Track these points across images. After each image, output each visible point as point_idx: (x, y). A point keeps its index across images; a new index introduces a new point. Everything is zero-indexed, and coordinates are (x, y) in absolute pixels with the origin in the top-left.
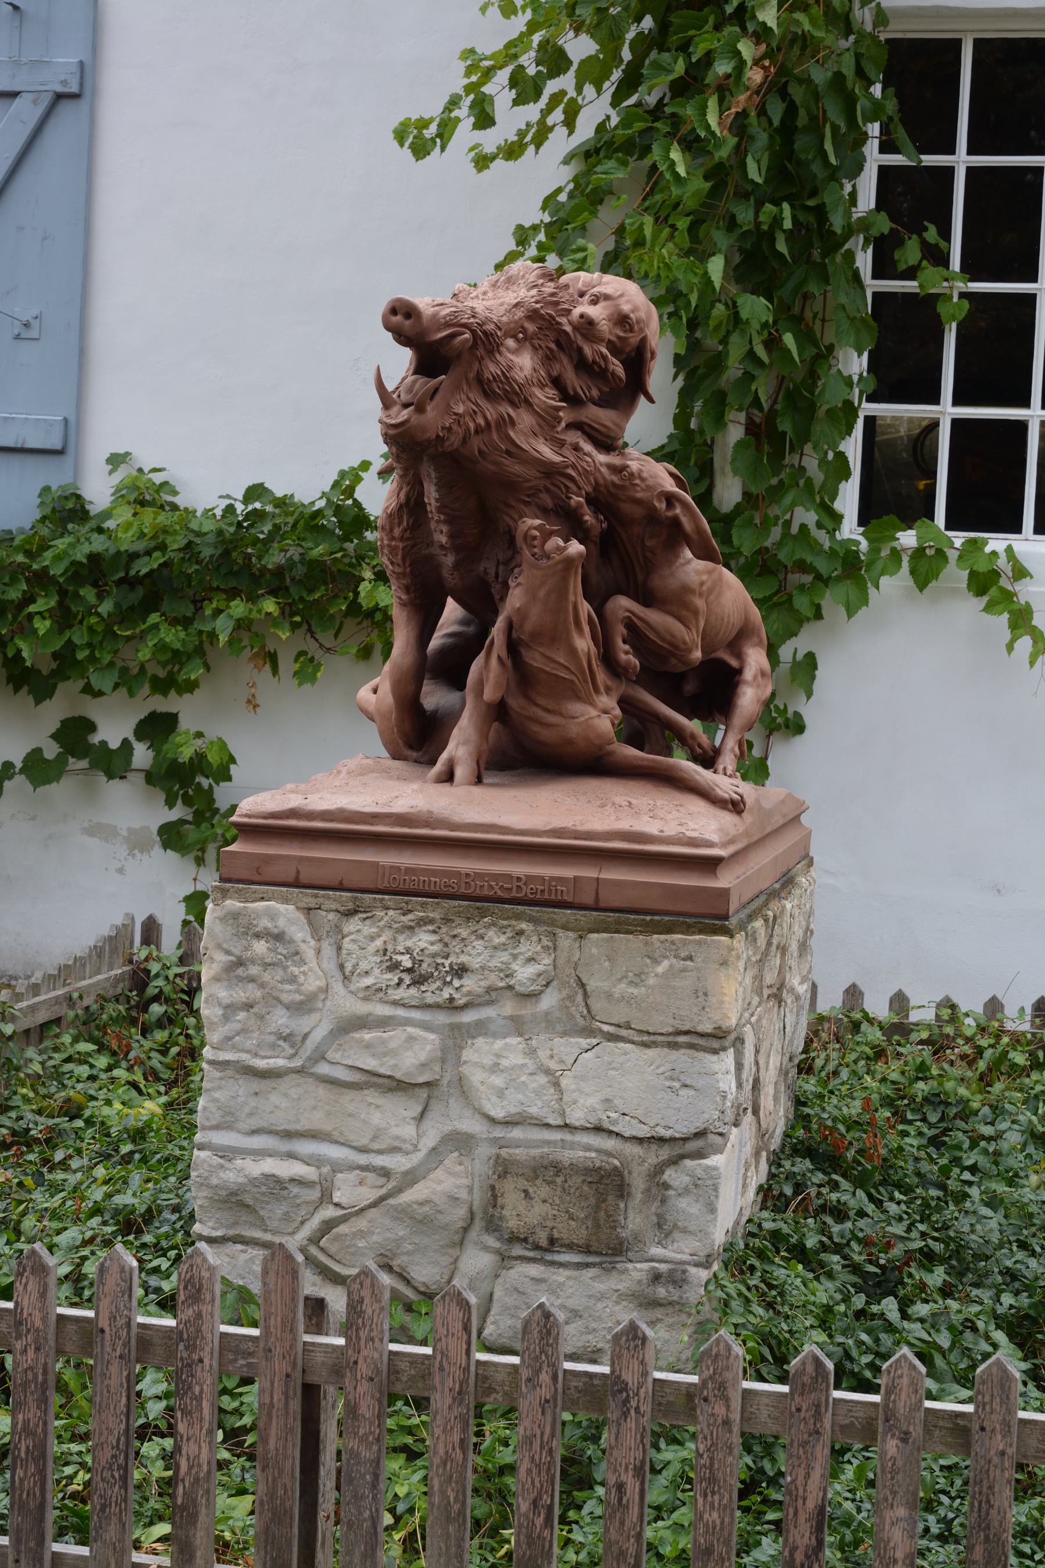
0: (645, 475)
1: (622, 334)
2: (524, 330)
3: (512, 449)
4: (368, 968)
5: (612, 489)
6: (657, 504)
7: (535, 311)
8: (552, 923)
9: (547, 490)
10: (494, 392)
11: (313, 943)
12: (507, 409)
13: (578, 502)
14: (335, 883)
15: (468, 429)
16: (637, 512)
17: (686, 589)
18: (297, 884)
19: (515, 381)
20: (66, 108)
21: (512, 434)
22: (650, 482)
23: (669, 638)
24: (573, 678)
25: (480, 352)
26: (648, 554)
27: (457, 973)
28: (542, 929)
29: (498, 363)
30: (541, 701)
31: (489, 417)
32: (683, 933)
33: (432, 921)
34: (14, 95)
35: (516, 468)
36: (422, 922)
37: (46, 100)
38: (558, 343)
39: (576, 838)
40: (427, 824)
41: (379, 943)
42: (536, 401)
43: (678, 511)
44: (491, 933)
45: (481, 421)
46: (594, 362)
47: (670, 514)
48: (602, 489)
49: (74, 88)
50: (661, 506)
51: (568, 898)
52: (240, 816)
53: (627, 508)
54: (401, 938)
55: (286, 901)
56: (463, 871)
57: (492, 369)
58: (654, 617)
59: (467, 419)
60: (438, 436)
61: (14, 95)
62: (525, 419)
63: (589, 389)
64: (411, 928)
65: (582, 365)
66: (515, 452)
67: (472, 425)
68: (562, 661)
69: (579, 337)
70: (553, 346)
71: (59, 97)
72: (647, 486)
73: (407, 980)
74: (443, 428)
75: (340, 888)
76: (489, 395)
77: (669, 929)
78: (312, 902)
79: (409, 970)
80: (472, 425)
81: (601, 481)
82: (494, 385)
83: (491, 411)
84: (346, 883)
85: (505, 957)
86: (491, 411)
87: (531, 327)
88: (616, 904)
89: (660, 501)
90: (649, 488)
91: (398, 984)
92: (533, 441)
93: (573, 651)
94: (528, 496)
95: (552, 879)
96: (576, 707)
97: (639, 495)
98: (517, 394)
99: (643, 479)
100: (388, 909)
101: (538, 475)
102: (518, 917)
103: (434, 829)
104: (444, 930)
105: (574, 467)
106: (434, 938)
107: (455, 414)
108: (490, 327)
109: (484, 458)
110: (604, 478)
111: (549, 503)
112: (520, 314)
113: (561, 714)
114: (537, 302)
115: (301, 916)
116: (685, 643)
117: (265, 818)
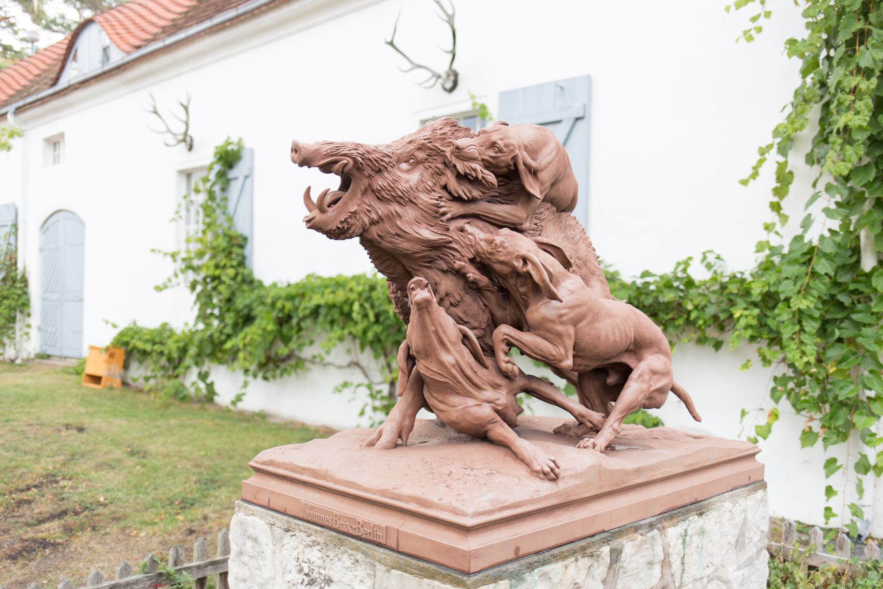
0: (506, 245)
1: (493, 155)
2: (415, 157)
3: (400, 233)
4: (290, 569)
5: (488, 256)
6: (516, 264)
7: (423, 145)
8: (373, 557)
9: (442, 259)
10: (383, 197)
11: (271, 546)
12: (395, 207)
13: (460, 265)
14: (283, 510)
15: (363, 222)
16: (506, 269)
17: (545, 319)
18: (268, 508)
19: (398, 189)
20: (580, 124)
21: (399, 223)
22: (510, 249)
23: (539, 352)
24: (447, 380)
25: (368, 171)
26: (524, 297)
27: (327, 583)
28: (368, 560)
29: (385, 178)
30: (435, 395)
31: (380, 213)
32: (440, 581)
33: (318, 544)
34: (559, 122)
35: (404, 245)
36: (315, 543)
37: (572, 121)
38: (445, 163)
39: (393, 498)
40: (324, 477)
41: (295, 554)
42: (420, 201)
43: (529, 267)
44: (345, 557)
45: (374, 216)
46: (466, 173)
47: (525, 270)
48: (483, 256)
49: (581, 115)
50: (519, 264)
51: (383, 541)
52: (256, 462)
53: (497, 267)
54: (307, 550)
55: (262, 518)
56: (335, 512)
57: (380, 182)
58: (527, 338)
59: (362, 215)
60: (338, 227)
61: (559, 122)
62: (409, 213)
63: (470, 192)
64: (311, 546)
65: (462, 177)
66: (401, 234)
67: (366, 220)
68: (435, 370)
69: (454, 158)
70: (440, 166)
71: (577, 119)
72: (508, 252)
73: (306, 579)
74: (342, 222)
75: (284, 513)
76: (381, 199)
77: (432, 576)
78: (272, 521)
79: (307, 575)
80: (366, 220)
81: (481, 251)
82: (383, 193)
83: (381, 209)
84: (288, 512)
85: (350, 575)
86: (381, 209)
87: (421, 155)
88: (407, 550)
89: (519, 261)
90: (509, 253)
91: (302, 583)
92: (415, 228)
93: (441, 364)
94: (429, 262)
95: (375, 526)
96: (455, 400)
97: (502, 258)
98: (401, 197)
99: (505, 248)
100: (301, 531)
101: (424, 248)
102: (357, 549)
103: (327, 481)
104: (324, 551)
105: (457, 242)
106: (319, 554)
107: (350, 212)
108: (373, 156)
109: (383, 240)
110: (482, 249)
111: (445, 267)
112: (412, 147)
113: (446, 404)
114: (425, 140)
115: (267, 528)
116: (553, 356)
117: (262, 464)
